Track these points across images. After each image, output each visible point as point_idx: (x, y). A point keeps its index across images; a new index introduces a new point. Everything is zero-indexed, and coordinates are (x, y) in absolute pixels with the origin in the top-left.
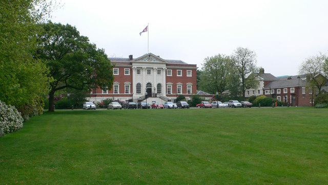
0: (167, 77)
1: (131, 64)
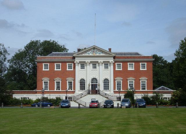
0: (115, 71)
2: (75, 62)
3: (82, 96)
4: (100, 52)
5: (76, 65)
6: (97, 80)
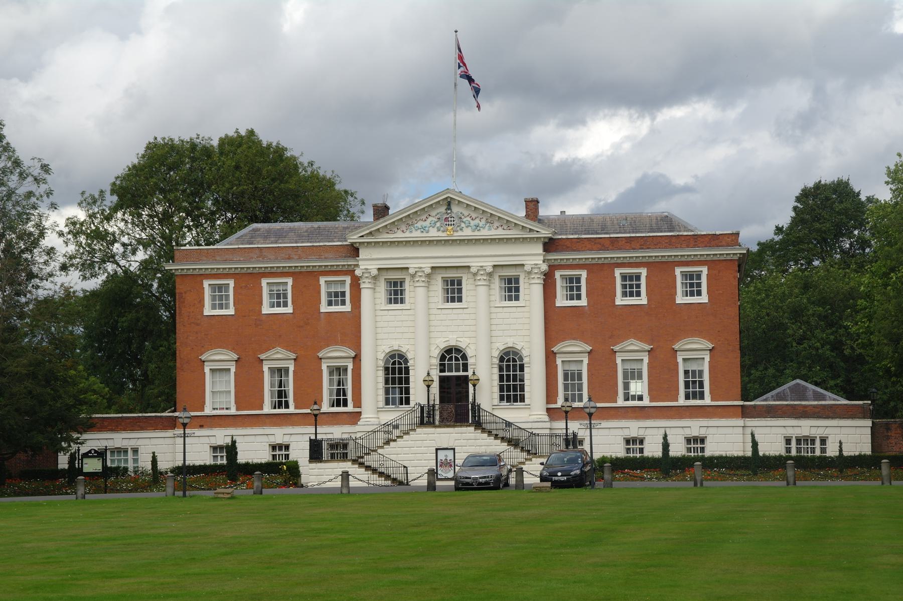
2: (358, 272)
3: (391, 434)
4: (477, 221)
5: (365, 285)
6: (464, 357)
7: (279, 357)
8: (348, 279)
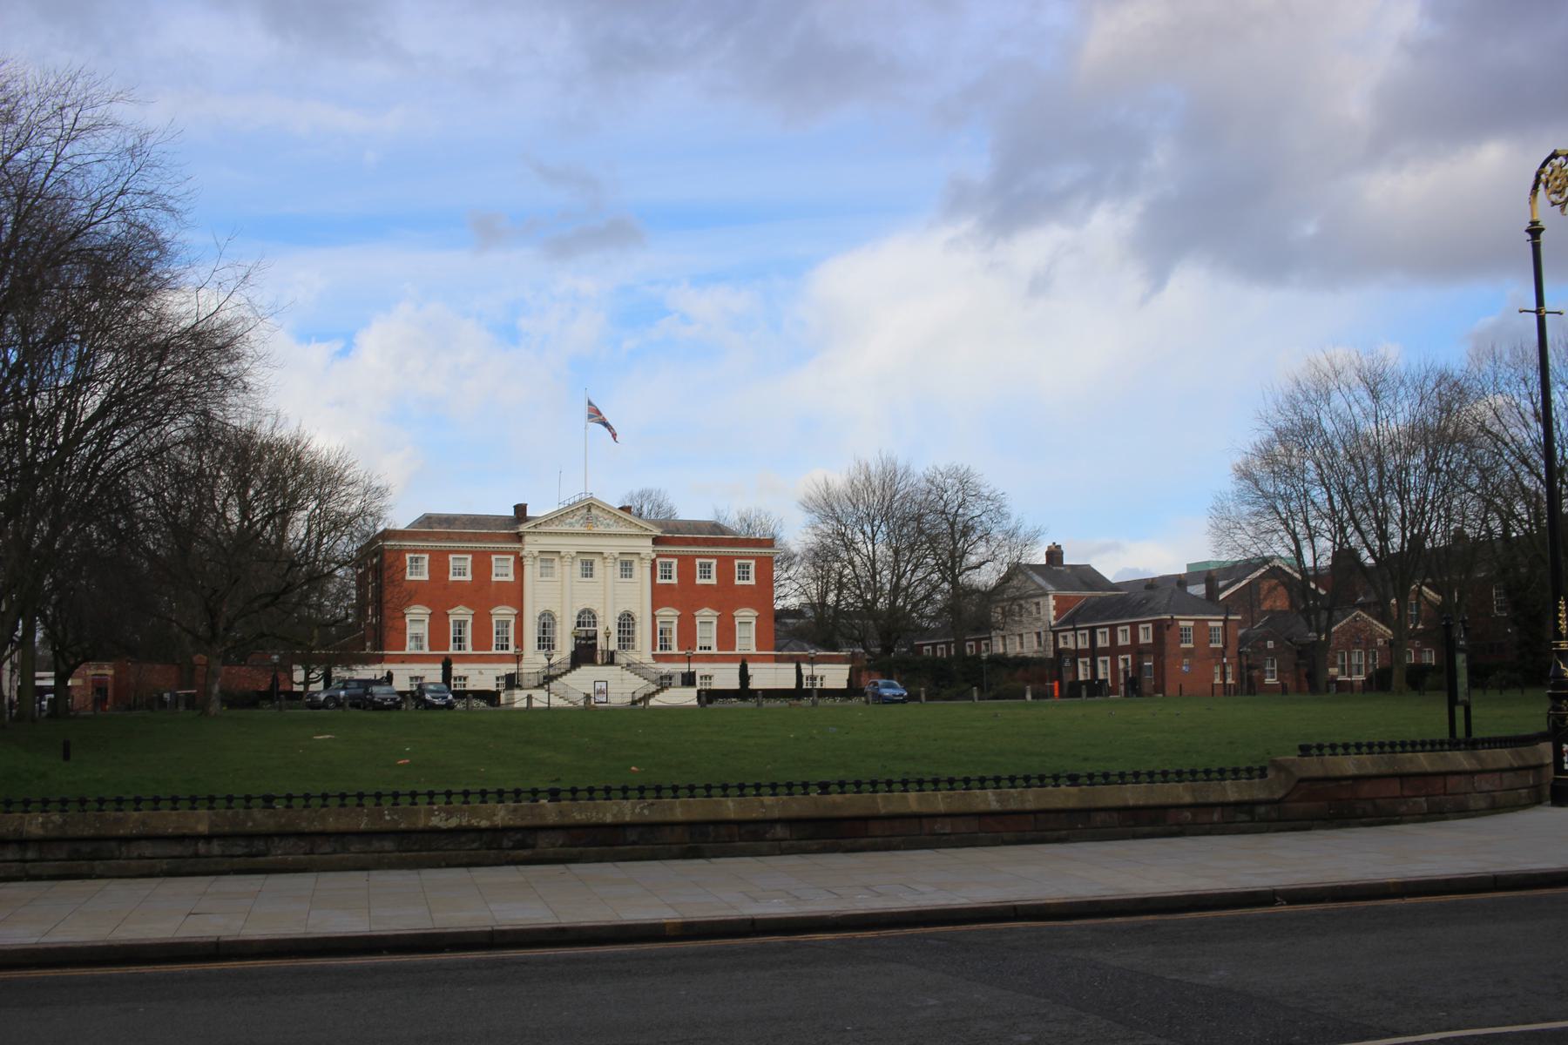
1: (519, 537)
2: (524, 553)
5: (527, 563)
7: (461, 614)
8: (512, 558)
